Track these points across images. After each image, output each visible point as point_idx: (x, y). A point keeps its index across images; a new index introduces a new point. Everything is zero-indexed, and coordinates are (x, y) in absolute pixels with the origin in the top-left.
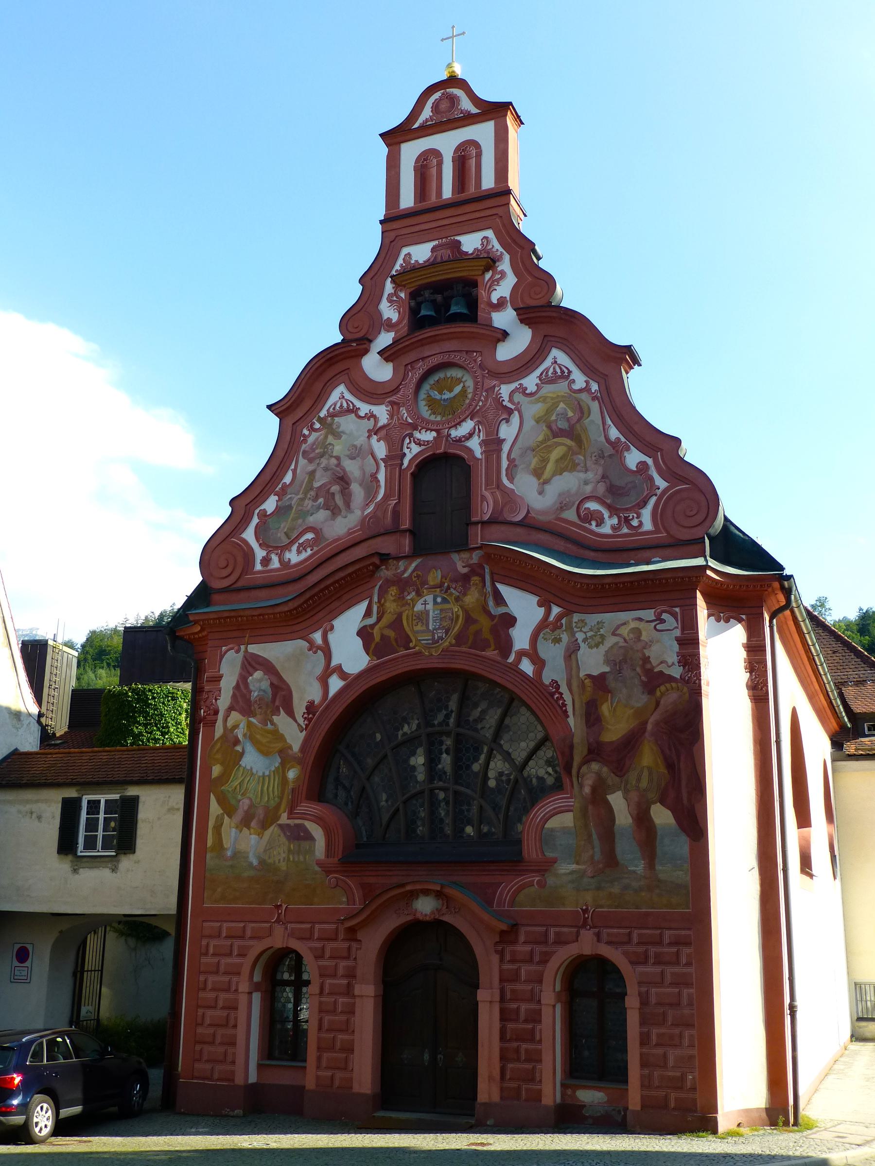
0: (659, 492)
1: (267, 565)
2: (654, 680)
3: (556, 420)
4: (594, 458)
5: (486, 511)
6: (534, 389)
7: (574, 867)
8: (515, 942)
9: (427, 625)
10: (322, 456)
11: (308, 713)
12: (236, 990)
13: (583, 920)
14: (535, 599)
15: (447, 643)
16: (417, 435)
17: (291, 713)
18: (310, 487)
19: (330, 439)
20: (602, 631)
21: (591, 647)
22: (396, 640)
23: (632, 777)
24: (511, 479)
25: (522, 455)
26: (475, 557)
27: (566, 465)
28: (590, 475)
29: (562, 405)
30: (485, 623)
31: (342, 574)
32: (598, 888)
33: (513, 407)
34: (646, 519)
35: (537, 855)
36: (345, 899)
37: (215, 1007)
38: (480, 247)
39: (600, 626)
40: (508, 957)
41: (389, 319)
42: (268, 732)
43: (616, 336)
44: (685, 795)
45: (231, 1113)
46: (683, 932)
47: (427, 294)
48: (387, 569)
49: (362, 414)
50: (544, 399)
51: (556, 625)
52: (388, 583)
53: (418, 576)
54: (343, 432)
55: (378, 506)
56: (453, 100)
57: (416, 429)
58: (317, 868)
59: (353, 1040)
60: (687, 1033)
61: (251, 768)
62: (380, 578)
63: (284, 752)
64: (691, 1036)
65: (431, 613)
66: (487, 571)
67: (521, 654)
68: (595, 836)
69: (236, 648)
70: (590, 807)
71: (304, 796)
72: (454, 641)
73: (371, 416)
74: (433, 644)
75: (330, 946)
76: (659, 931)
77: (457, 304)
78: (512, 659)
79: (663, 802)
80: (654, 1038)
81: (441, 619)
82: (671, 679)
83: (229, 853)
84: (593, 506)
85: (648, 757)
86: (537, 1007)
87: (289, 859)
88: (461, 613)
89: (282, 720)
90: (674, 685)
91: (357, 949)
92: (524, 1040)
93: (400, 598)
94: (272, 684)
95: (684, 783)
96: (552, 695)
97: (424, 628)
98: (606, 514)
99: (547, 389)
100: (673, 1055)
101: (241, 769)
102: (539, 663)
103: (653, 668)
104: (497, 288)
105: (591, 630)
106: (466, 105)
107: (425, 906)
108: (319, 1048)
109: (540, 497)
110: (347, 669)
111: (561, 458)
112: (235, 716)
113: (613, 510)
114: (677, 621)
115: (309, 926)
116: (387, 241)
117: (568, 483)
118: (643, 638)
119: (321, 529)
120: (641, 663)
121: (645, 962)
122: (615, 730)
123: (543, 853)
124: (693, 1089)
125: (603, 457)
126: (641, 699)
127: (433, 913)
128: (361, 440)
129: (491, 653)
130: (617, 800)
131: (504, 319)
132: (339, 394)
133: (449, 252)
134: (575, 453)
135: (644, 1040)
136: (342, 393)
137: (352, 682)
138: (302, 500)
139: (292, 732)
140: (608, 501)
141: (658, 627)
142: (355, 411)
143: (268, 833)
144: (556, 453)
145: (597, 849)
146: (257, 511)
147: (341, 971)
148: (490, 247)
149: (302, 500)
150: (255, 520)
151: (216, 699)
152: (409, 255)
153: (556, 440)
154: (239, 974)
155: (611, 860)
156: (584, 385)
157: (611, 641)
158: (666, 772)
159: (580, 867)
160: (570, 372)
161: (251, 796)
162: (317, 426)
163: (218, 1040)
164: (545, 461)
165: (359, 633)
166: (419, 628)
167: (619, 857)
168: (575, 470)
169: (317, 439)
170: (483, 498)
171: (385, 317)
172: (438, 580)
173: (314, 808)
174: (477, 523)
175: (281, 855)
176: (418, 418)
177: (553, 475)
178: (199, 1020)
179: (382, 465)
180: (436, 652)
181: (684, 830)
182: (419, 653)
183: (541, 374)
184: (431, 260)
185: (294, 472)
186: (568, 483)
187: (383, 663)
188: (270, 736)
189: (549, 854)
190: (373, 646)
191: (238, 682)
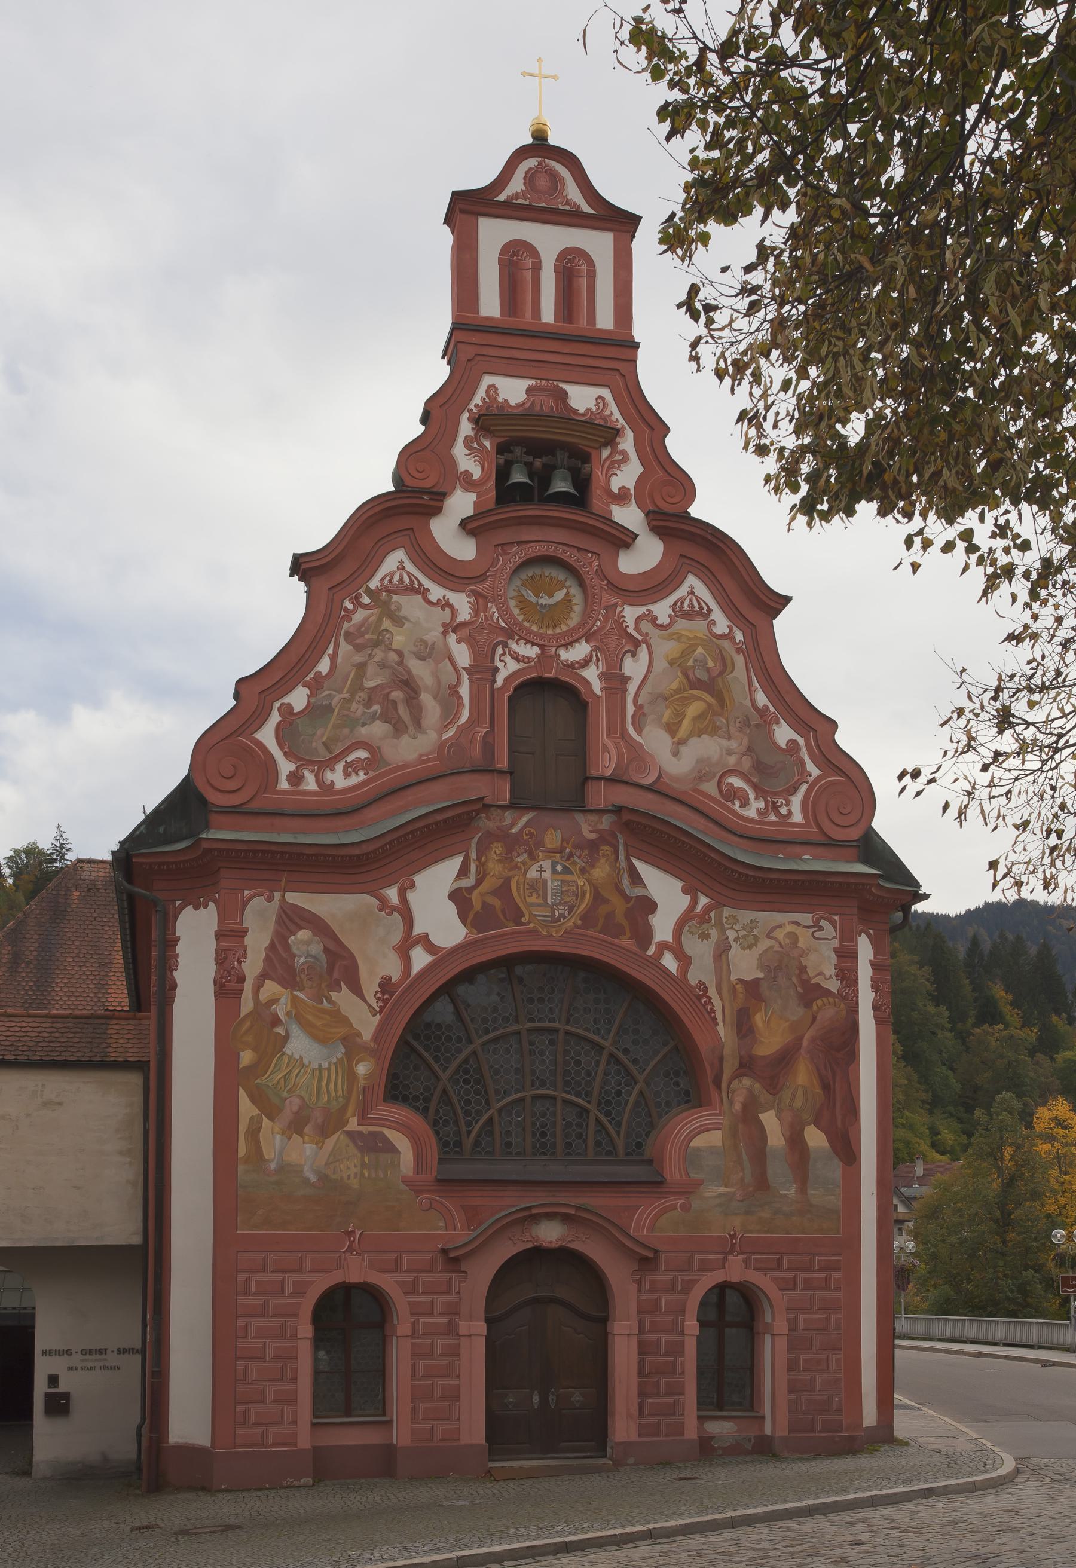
0: (810, 779)
1: (298, 784)
2: (811, 993)
4: (738, 725)
6: (667, 621)
7: (722, 1189)
9: (545, 899)
10: (376, 644)
11: (383, 993)
12: (294, 1336)
13: (729, 1246)
14: (679, 884)
15: (571, 924)
16: (513, 645)
17: (357, 991)
18: (357, 686)
19: (387, 624)
20: (755, 932)
21: (743, 948)
22: (503, 912)
24: (639, 730)
27: (705, 726)
28: (733, 744)
29: (700, 650)
30: (619, 907)
33: (640, 638)
35: (681, 1176)
36: (442, 1224)
37: (263, 1358)
38: (594, 409)
39: (753, 925)
40: (646, 1287)
42: (325, 1012)
43: (776, 582)
45: (296, 1483)
47: (518, 451)
49: (433, 598)
50: (679, 638)
51: (704, 918)
54: (406, 618)
55: (462, 730)
56: (556, 181)
58: (403, 1187)
59: (459, 1386)
61: (301, 1058)
65: (549, 883)
67: (663, 947)
68: (745, 1157)
69: (267, 894)
71: (381, 1096)
72: (579, 922)
73: (445, 604)
74: (552, 922)
76: (807, 1257)
77: (564, 479)
78: (651, 951)
80: (801, 1363)
81: (563, 892)
82: (828, 993)
83: (273, 1166)
84: (737, 782)
85: (803, 1075)
87: (362, 1174)
88: (588, 888)
89: (343, 998)
91: (460, 1282)
93: (507, 858)
94: (326, 950)
95: (838, 1105)
96: (699, 998)
97: (540, 901)
98: (752, 796)
99: (682, 625)
101: (286, 1059)
102: (684, 960)
104: (618, 472)
105: (743, 929)
107: (550, 1234)
108: (413, 1399)
110: (434, 939)
112: (271, 988)
113: (761, 792)
115: (394, 1256)
118: (799, 945)
119: (379, 748)
120: (797, 972)
121: (794, 1288)
122: (770, 1041)
123: (688, 1175)
124: (839, 1410)
125: (749, 726)
126: (797, 1012)
127: (558, 1240)
128: (434, 635)
129: (625, 941)
130: (769, 1119)
132: (395, 562)
133: (551, 402)
135: (792, 1366)
136: (402, 562)
137: (442, 957)
139: (364, 1019)
140: (755, 780)
141: (816, 934)
142: (423, 592)
143: (330, 1143)
144: (694, 709)
146: (277, 705)
148: (607, 413)
150: (275, 718)
151: (240, 962)
152: (492, 388)
153: (693, 692)
154: (296, 1316)
155: (762, 1183)
156: (727, 631)
157: (765, 944)
159: (726, 1190)
160: (709, 610)
161: (303, 1093)
162: (366, 600)
164: (680, 716)
166: (533, 899)
169: (366, 619)
170: (605, 748)
172: (557, 844)
174: (598, 779)
175: (351, 1168)
177: (691, 735)
179: (465, 676)
180: (557, 932)
182: (534, 932)
183: (675, 604)
184: (527, 405)
185: (333, 658)
188: (328, 1017)
190: (471, 915)
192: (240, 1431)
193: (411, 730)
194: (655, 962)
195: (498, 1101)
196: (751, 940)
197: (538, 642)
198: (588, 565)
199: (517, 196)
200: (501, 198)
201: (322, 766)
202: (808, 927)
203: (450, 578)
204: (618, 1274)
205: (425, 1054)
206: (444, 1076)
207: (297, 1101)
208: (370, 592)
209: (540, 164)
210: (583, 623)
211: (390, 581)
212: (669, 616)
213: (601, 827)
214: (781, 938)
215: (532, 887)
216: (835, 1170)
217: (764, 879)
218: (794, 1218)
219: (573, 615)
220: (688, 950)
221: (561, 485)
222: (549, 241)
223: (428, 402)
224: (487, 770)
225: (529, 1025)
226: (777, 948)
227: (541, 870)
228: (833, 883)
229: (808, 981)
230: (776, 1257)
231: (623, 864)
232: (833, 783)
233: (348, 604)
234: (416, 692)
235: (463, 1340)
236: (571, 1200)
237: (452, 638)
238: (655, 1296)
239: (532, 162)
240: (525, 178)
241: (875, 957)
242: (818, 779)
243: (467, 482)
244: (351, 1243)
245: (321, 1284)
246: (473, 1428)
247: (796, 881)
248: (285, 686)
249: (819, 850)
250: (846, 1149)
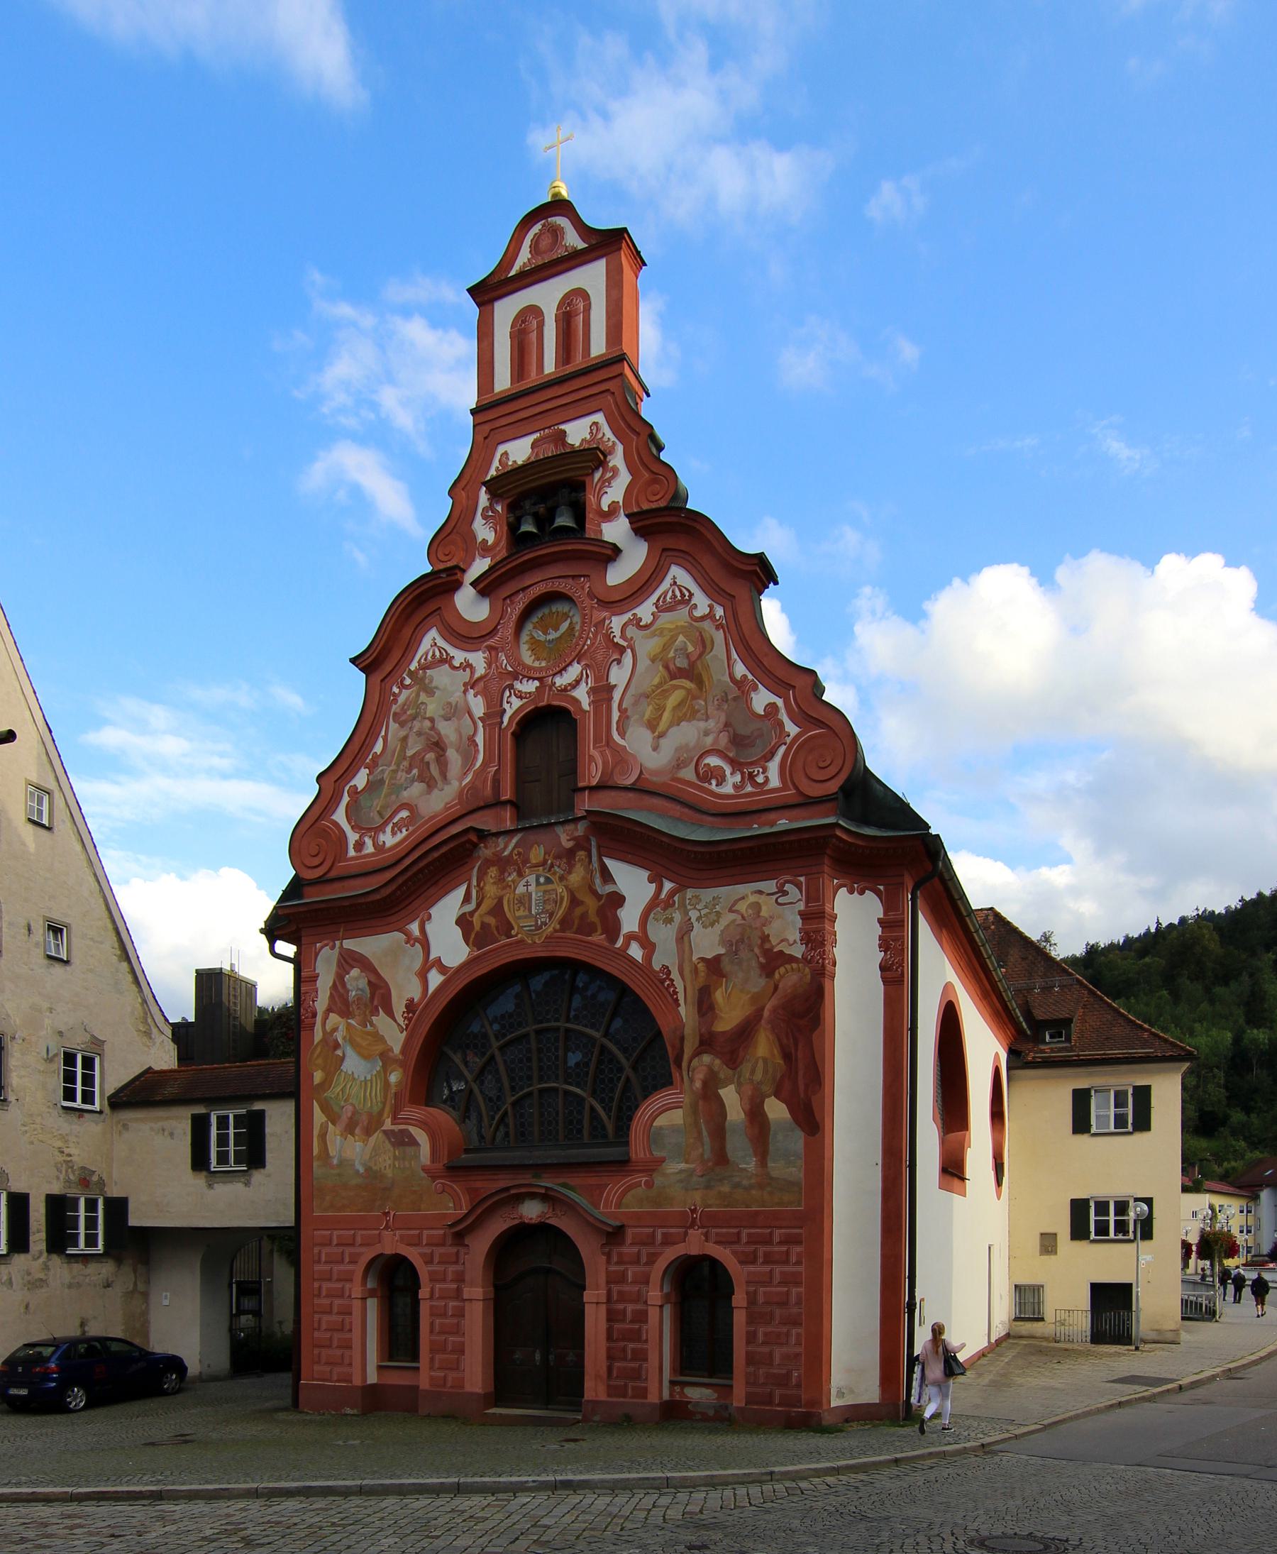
2: (773, 961)
3: (674, 658)
5: (593, 774)
7: (683, 1166)
8: (622, 1243)
14: (645, 874)
15: (551, 929)
17: (390, 1013)
22: (497, 928)
23: (746, 1069)
24: (622, 734)
25: (636, 703)
26: (580, 829)
27: (685, 713)
28: (711, 724)
30: (591, 905)
31: (436, 855)
32: (708, 1187)
34: (773, 775)
40: (615, 1259)
42: (368, 1033)
44: (802, 1087)
48: (486, 847)
52: (488, 863)
53: (519, 854)
58: (423, 1174)
63: (385, 1056)
65: (534, 895)
67: (630, 937)
70: (701, 1103)
75: (439, 1251)
78: (619, 944)
79: (777, 1095)
82: (792, 959)
83: (335, 1161)
84: (713, 761)
85: (764, 1047)
88: (565, 894)
89: (381, 1020)
90: (794, 965)
93: (501, 880)
94: (369, 982)
95: (801, 1073)
96: (662, 982)
98: (728, 771)
102: (649, 947)
103: (773, 947)
105: (706, 907)
111: (679, 705)
112: (334, 1018)
113: (736, 765)
118: (764, 913)
122: (729, 1016)
123: (651, 1153)
126: (758, 983)
129: (598, 938)
130: (730, 1095)
134: (694, 698)
137: (451, 975)
140: (731, 755)
143: (372, 1140)
144: (672, 701)
145: (707, 1147)
153: (674, 682)
155: (721, 1158)
157: (728, 918)
158: (782, 1062)
164: (660, 709)
165: (457, 923)
166: (521, 913)
167: (730, 1154)
170: (592, 758)
173: (417, 1112)
174: (584, 789)
175: (387, 1161)
182: (522, 941)
187: (485, 954)
191: (334, 983)
194: (623, 954)
196: (713, 917)
204: (588, 1248)
213: (577, 834)
215: (520, 902)
216: (797, 1141)
218: (754, 1192)
220: (653, 938)
226: (740, 921)
227: (527, 885)
229: (770, 950)
230: (735, 1230)
231: (595, 864)
238: (622, 1268)
241: (885, 914)
244: (388, 1222)
249: (795, 812)
250: (812, 1118)
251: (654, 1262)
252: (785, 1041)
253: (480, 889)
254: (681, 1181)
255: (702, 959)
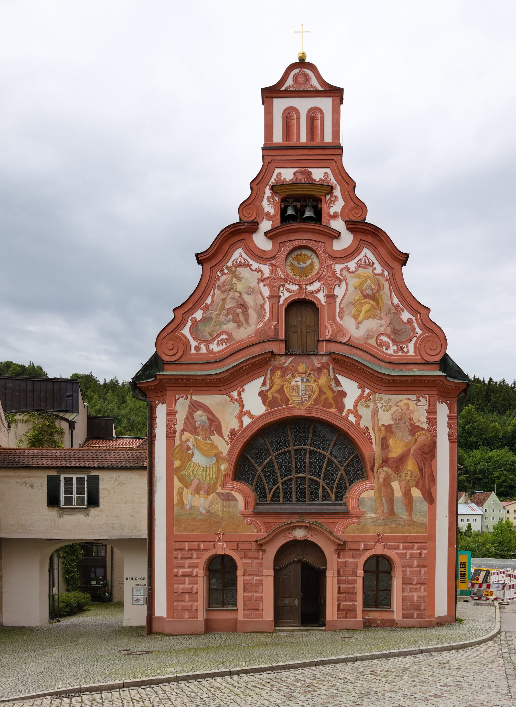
0: (417, 335)
1: (198, 351)
2: (415, 429)
6: (354, 270)
7: (374, 515)
8: (345, 549)
10: (230, 290)
11: (231, 436)
12: (196, 575)
13: (378, 539)
14: (356, 384)
15: (309, 403)
16: (287, 285)
17: (221, 435)
18: (223, 308)
19: (235, 281)
20: (390, 404)
21: (384, 411)
22: (281, 400)
23: (403, 474)
24: (341, 318)
25: (348, 306)
27: (371, 315)
28: (383, 322)
29: (369, 281)
30: (330, 395)
32: (385, 525)
33: (342, 278)
34: (411, 349)
36: (255, 530)
38: (323, 178)
40: (341, 556)
41: (268, 213)
42: (208, 444)
46: (423, 544)
47: (291, 201)
48: (275, 361)
49: (254, 268)
50: (359, 277)
54: (242, 278)
55: (266, 324)
57: (286, 282)
58: (239, 515)
60: (423, 587)
62: (271, 365)
63: (218, 456)
64: (425, 588)
66: (331, 367)
67: (349, 412)
68: (384, 501)
69: (185, 397)
70: (382, 488)
72: (313, 403)
73: (259, 270)
75: (248, 553)
77: (309, 211)
78: (344, 414)
80: (409, 590)
81: (306, 391)
82: (423, 429)
83: (188, 507)
84: (384, 338)
85: (411, 465)
86: (355, 578)
88: (317, 388)
89: (215, 438)
90: (424, 432)
91: (263, 554)
92: (348, 593)
93: (283, 377)
94: (208, 418)
95: (426, 478)
98: (391, 344)
99: (361, 271)
100: (416, 596)
101: (193, 463)
102: (358, 417)
104: (333, 205)
105: (385, 402)
106: (315, 83)
107: (300, 534)
109: (357, 330)
112: (186, 435)
114: (426, 401)
116: (267, 163)
117: (372, 324)
118: (411, 408)
119: (231, 333)
120: (409, 420)
122: (395, 452)
126: (408, 438)
128: (254, 284)
129: (333, 410)
130: (395, 485)
131: (338, 225)
132: (238, 254)
133: (304, 177)
134: (375, 309)
135: (404, 590)
136: (241, 253)
137: (256, 420)
138: (219, 315)
139: (223, 446)
140: (392, 337)
142: (249, 266)
143: (210, 497)
145: (385, 508)
146: (190, 318)
147: (254, 564)
148: (329, 179)
149: (219, 315)
150: (189, 324)
151: (174, 425)
152: (279, 174)
153: (365, 300)
154: (197, 567)
155: (392, 512)
158: (418, 472)
160: (373, 263)
161: (199, 477)
162: (226, 271)
163: (187, 599)
164: (359, 311)
167: (395, 511)
168: (375, 318)
169: (226, 280)
171: (266, 211)
173: (237, 485)
174: (323, 341)
175: (219, 507)
176: (288, 276)
177: (364, 320)
178: (176, 591)
179: (267, 300)
181: (425, 499)
183: (358, 262)
184: (294, 180)
185: (213, 297)
186: (372, 324)
189: (362, 509)
190: (268, 402)
191: (187, 416)
192: (175, 612)
193: (245, 325)
194: (346, 419)
195: (282, 479)
197: (298, 283)
198: (320, 248)
199: (290, 87)
200: (283, 89)
201: (208, 342)
202: (414, 401)
203: (261, 259)
204: (329, 551)
205: (252, 460)
206: (259, 469)
207: (197, 481)
208: (227, 268)
209: (300, 71)
210: (318, 273)
211: (236, 262)
212: (355, 267)
213: (323, 362)
214: (402, 406)
215: (293, 389)
216: (425, 506)
217: (393, 380)
219: (314, 270)
221: (308, 213)
222: (303, 105)
223: (251, 184)
224: (275, 340)
225: (294, 447)
226: (400, 410)
228: (424, 381)
230: (398, 544)
231: (332, 376)
232: (428, 336)
233: (219, 274)
234: (246, 309)
235: (264, 577)
236: (309, 520)
237: (262, 284)
239: (296, 71)
240: (293, 78)
242: (421, 335)
243: (269, 216)
244: (219, 538)
245: (207, 555)
246: (268, 614)
247: (408, 381)
248: (193, 310)
249: (421, 367)
250: (430, 497)
251: (360, 558)
252: (420, 464)
253: (272, 380)
254: (373, 522)
255: (383, 425)
